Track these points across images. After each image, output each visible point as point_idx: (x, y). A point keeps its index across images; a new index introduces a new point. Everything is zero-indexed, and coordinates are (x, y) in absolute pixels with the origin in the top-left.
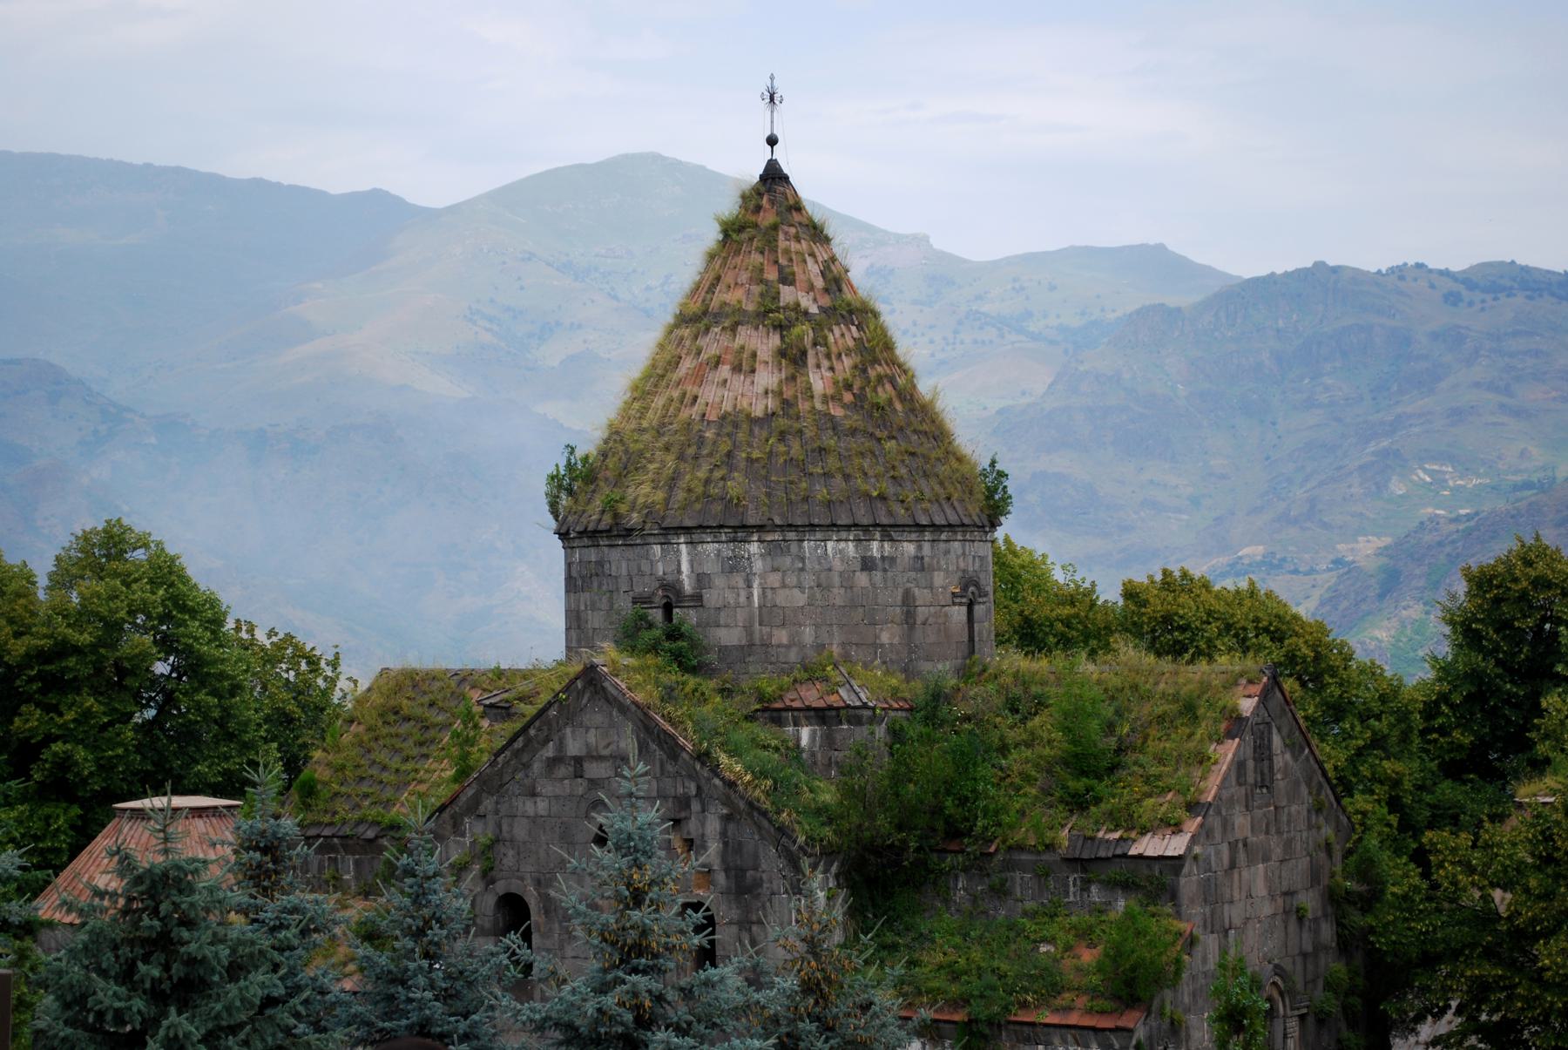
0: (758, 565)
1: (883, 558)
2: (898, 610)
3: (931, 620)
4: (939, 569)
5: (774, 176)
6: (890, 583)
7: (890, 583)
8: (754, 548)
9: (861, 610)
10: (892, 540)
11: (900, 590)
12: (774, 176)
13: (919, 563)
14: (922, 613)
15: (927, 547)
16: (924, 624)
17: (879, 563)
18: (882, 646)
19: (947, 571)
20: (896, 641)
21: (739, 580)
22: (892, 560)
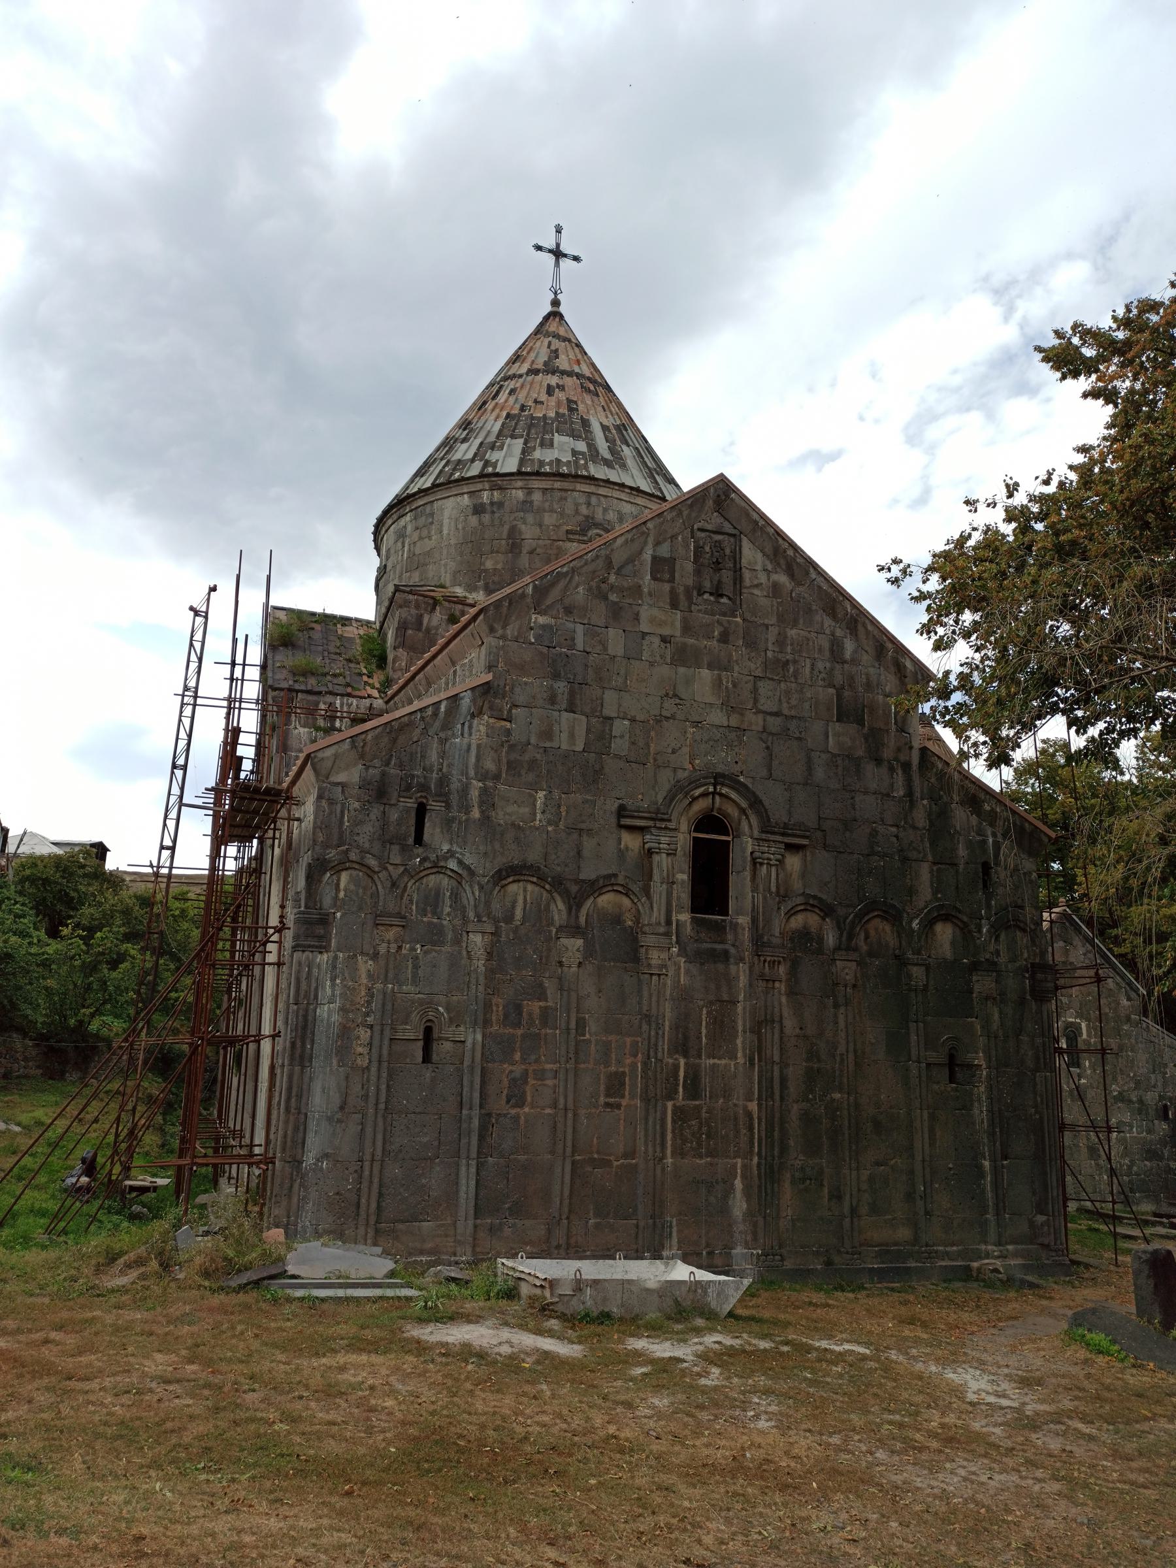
0: (409, 528)
1: (492, 504)
2: (503, 542)
3: (539, 550)
4: (552, 511)
5: (555, 315)
6: (497, 522)
7: (497, 522)
8: (408, 518)
9: (470, 545)
10: (500, 488)
11: (507, 527)
12: (555, 315)
13: (526, 506)
14: (527, 546)
15: (537, 497)
16: (531, 552)
17: (488, 508)
18: (486, 571)
19: (562, 514)
20: (499, 566)
21: (399, 544)
22: (500, 505)
